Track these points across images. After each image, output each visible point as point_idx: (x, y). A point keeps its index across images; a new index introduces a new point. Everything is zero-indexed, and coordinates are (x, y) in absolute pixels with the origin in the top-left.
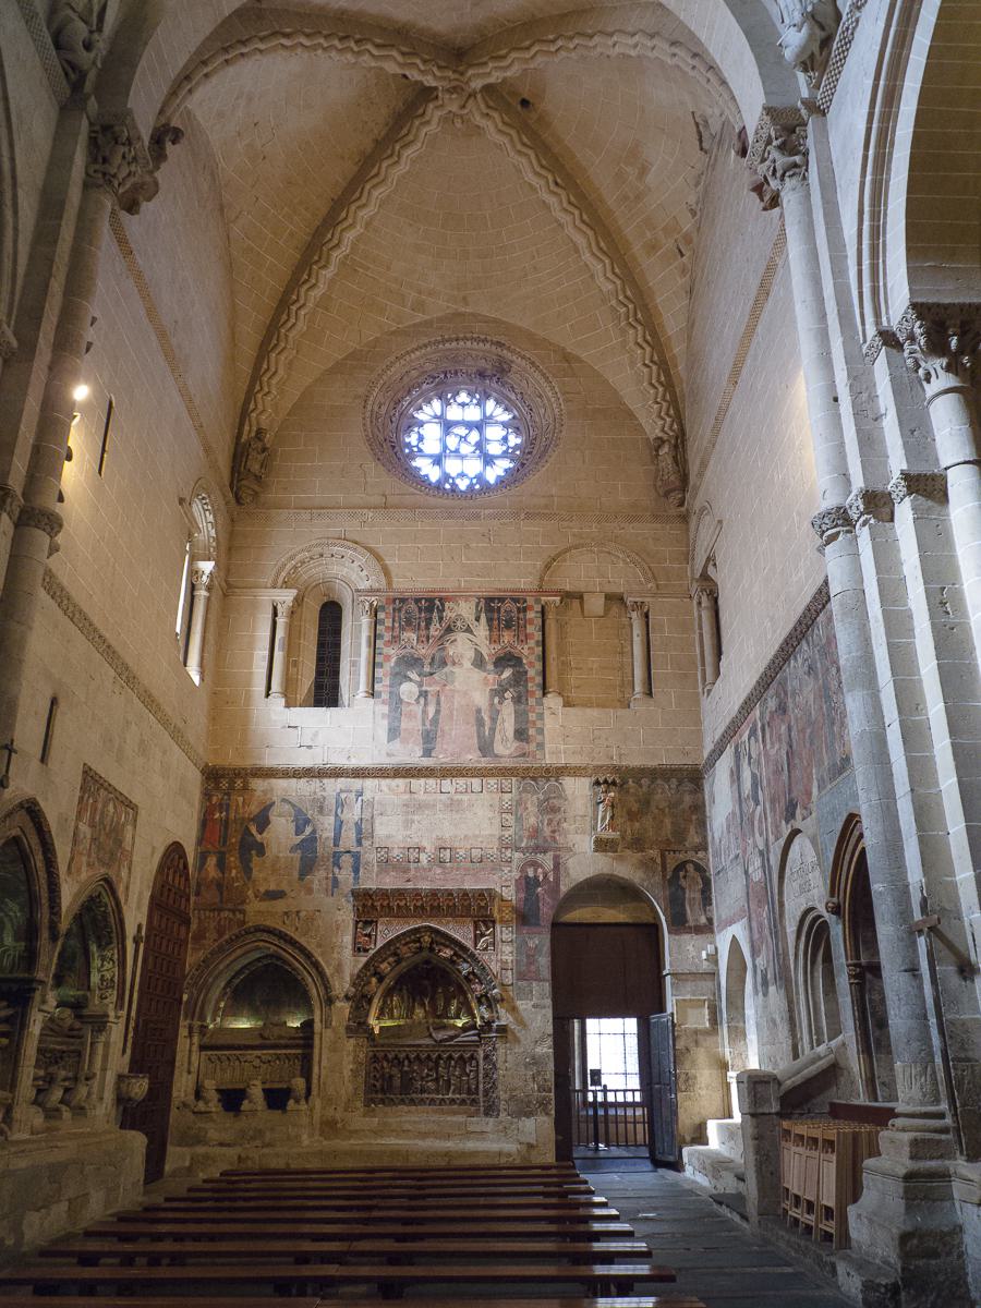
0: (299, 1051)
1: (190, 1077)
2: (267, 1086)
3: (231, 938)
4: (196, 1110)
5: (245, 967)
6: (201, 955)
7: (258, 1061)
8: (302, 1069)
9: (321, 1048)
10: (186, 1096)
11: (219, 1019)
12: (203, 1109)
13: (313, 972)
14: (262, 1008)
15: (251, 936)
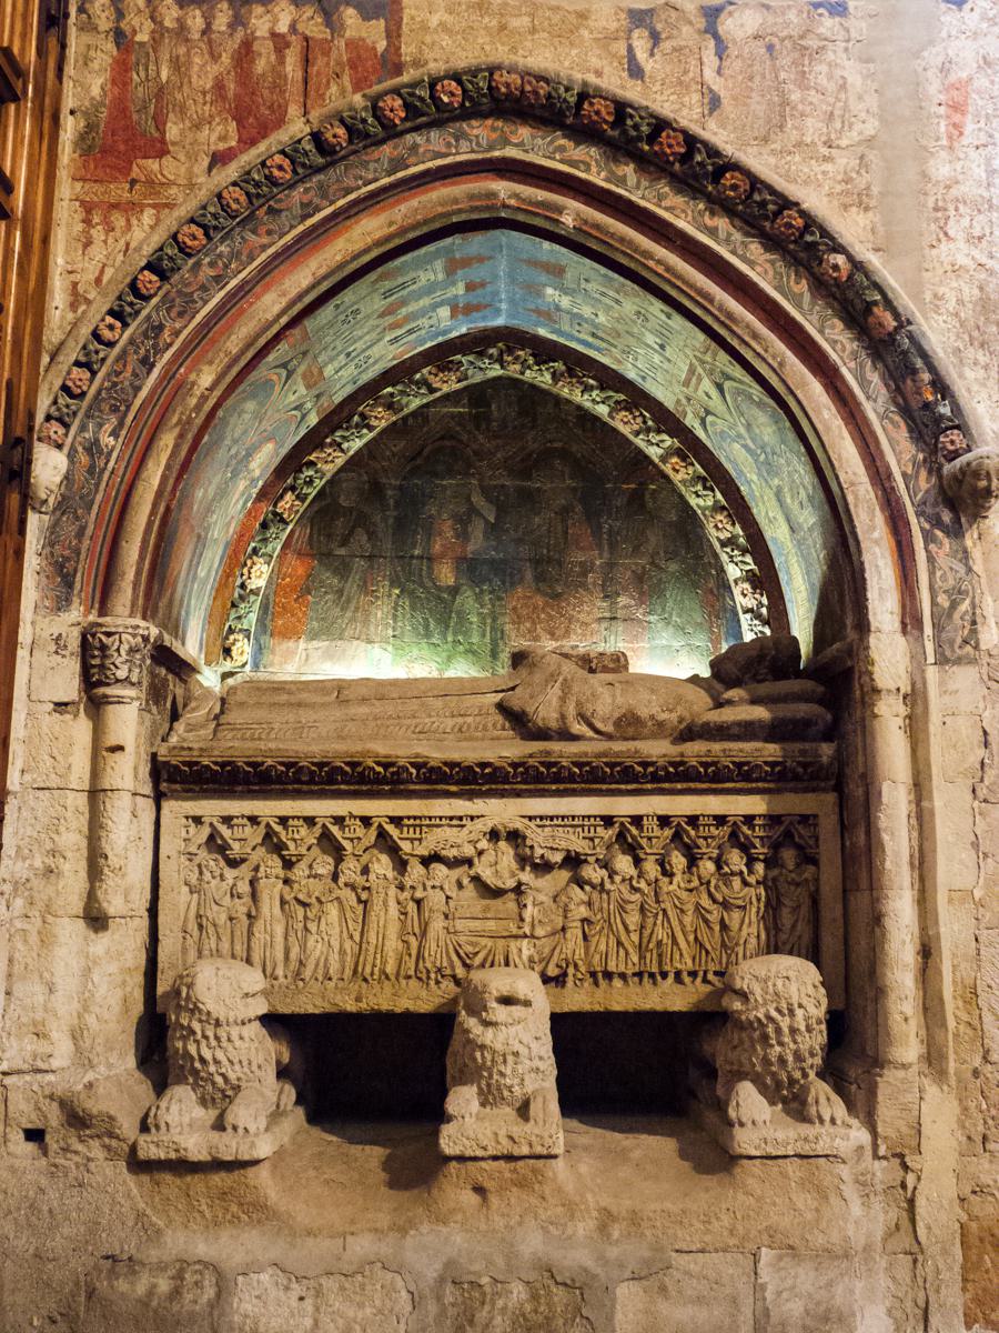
0: (755, 805)
1: (101, 944)
2: (579, 999)
3: (316, 137)
4: (150, 1150)
5: (369, 391)
6: (145, 234)
7: (506, 851)
8: (773, 907)
9: (920, 787)
10: (83, 1059)
11: (243, 649)
12: (196, 1146)
13: (836, 341)
14: (467, 599)
15: (436, 139)
